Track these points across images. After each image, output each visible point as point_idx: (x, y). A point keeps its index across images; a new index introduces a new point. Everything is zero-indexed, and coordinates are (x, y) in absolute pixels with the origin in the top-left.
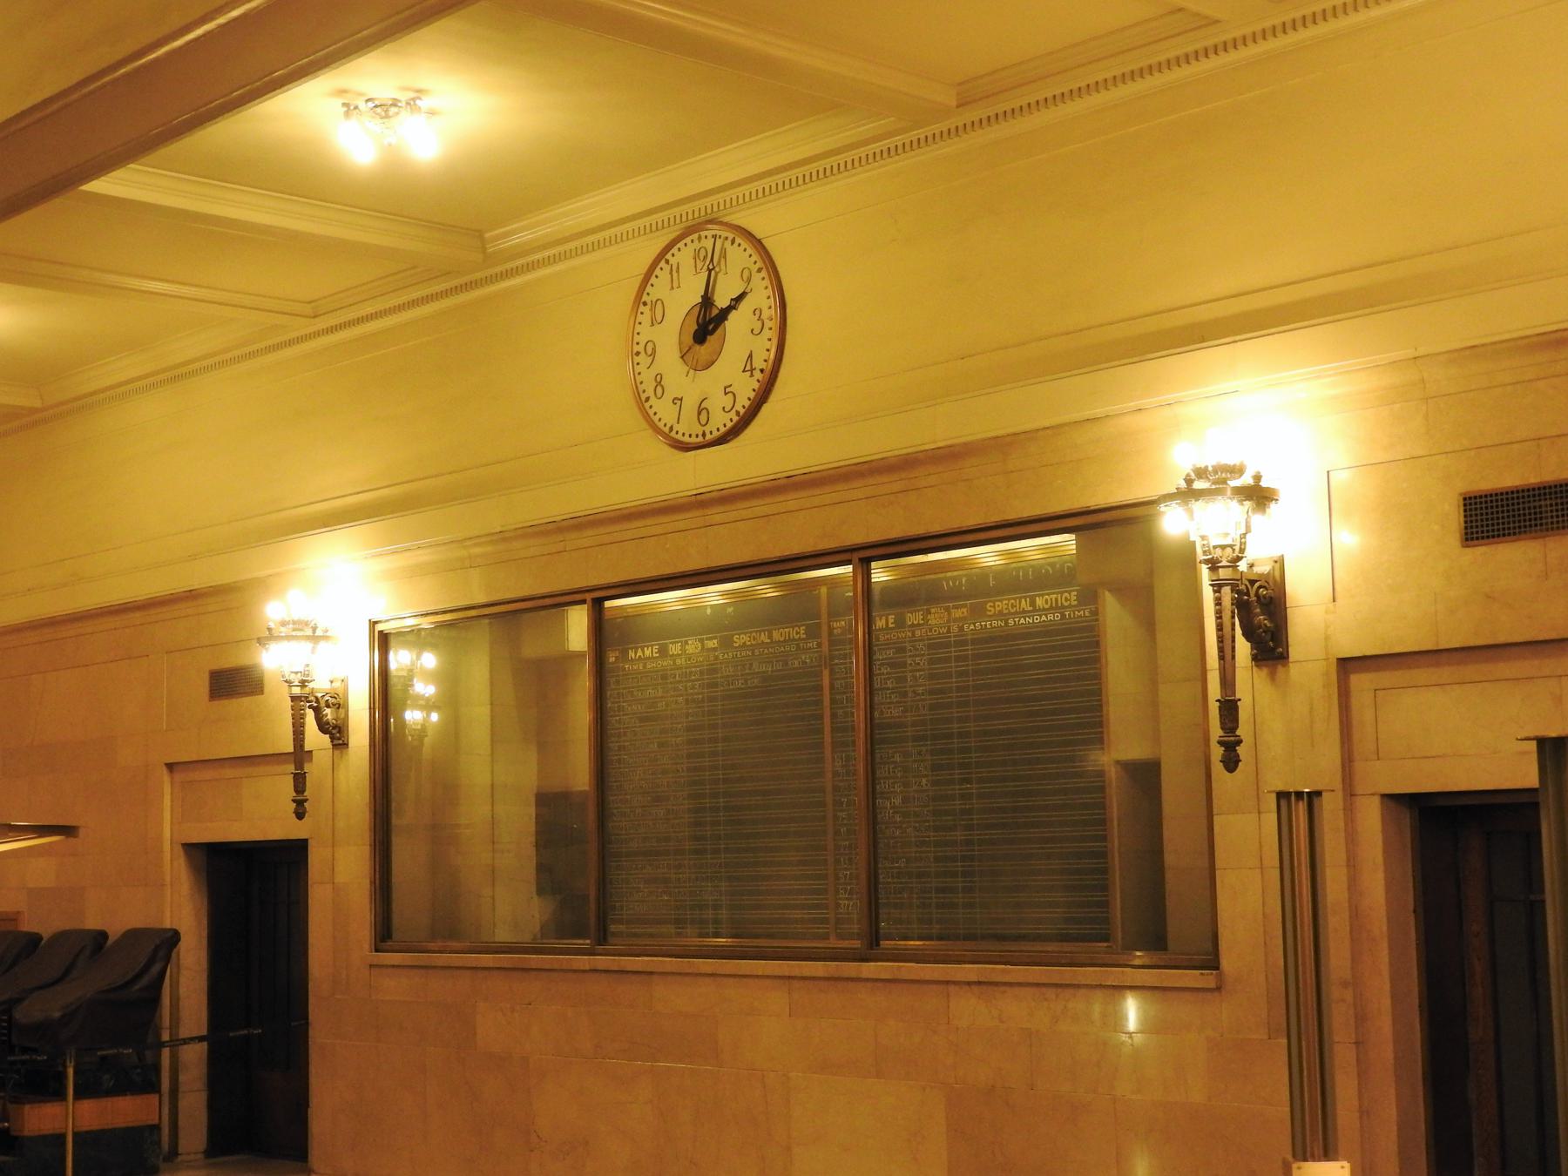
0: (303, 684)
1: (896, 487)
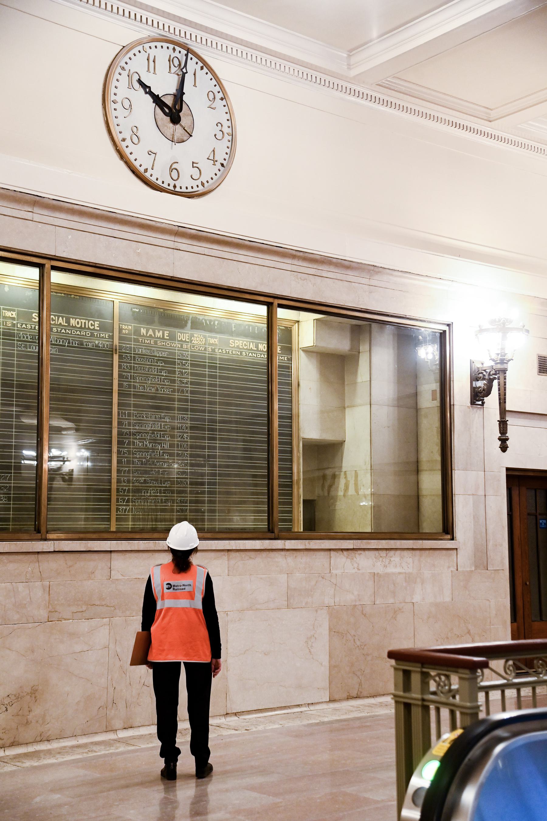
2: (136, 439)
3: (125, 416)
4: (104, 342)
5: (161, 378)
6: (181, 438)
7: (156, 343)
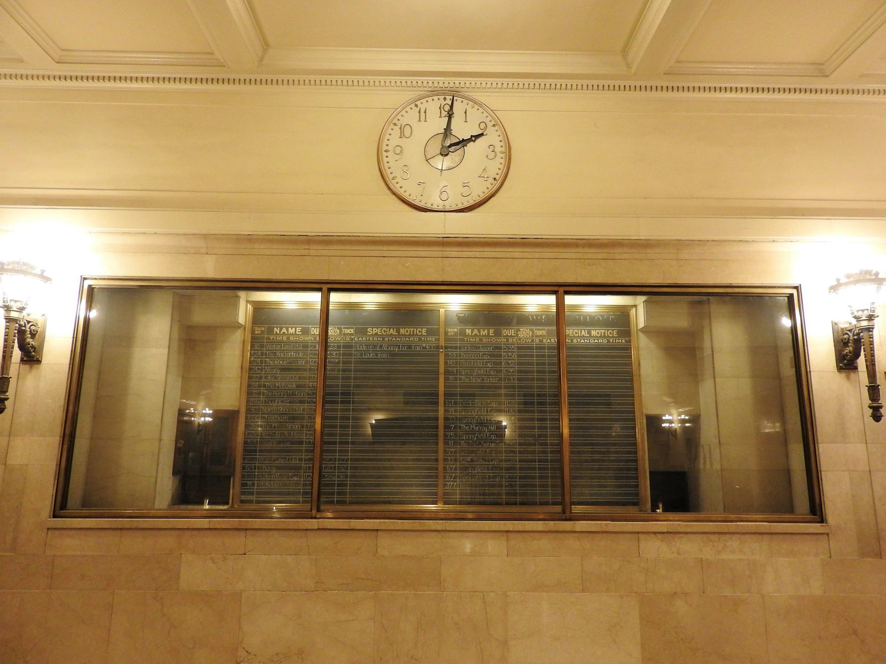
0: (21, 309)
1: (601, 256)
7: (481, 340)
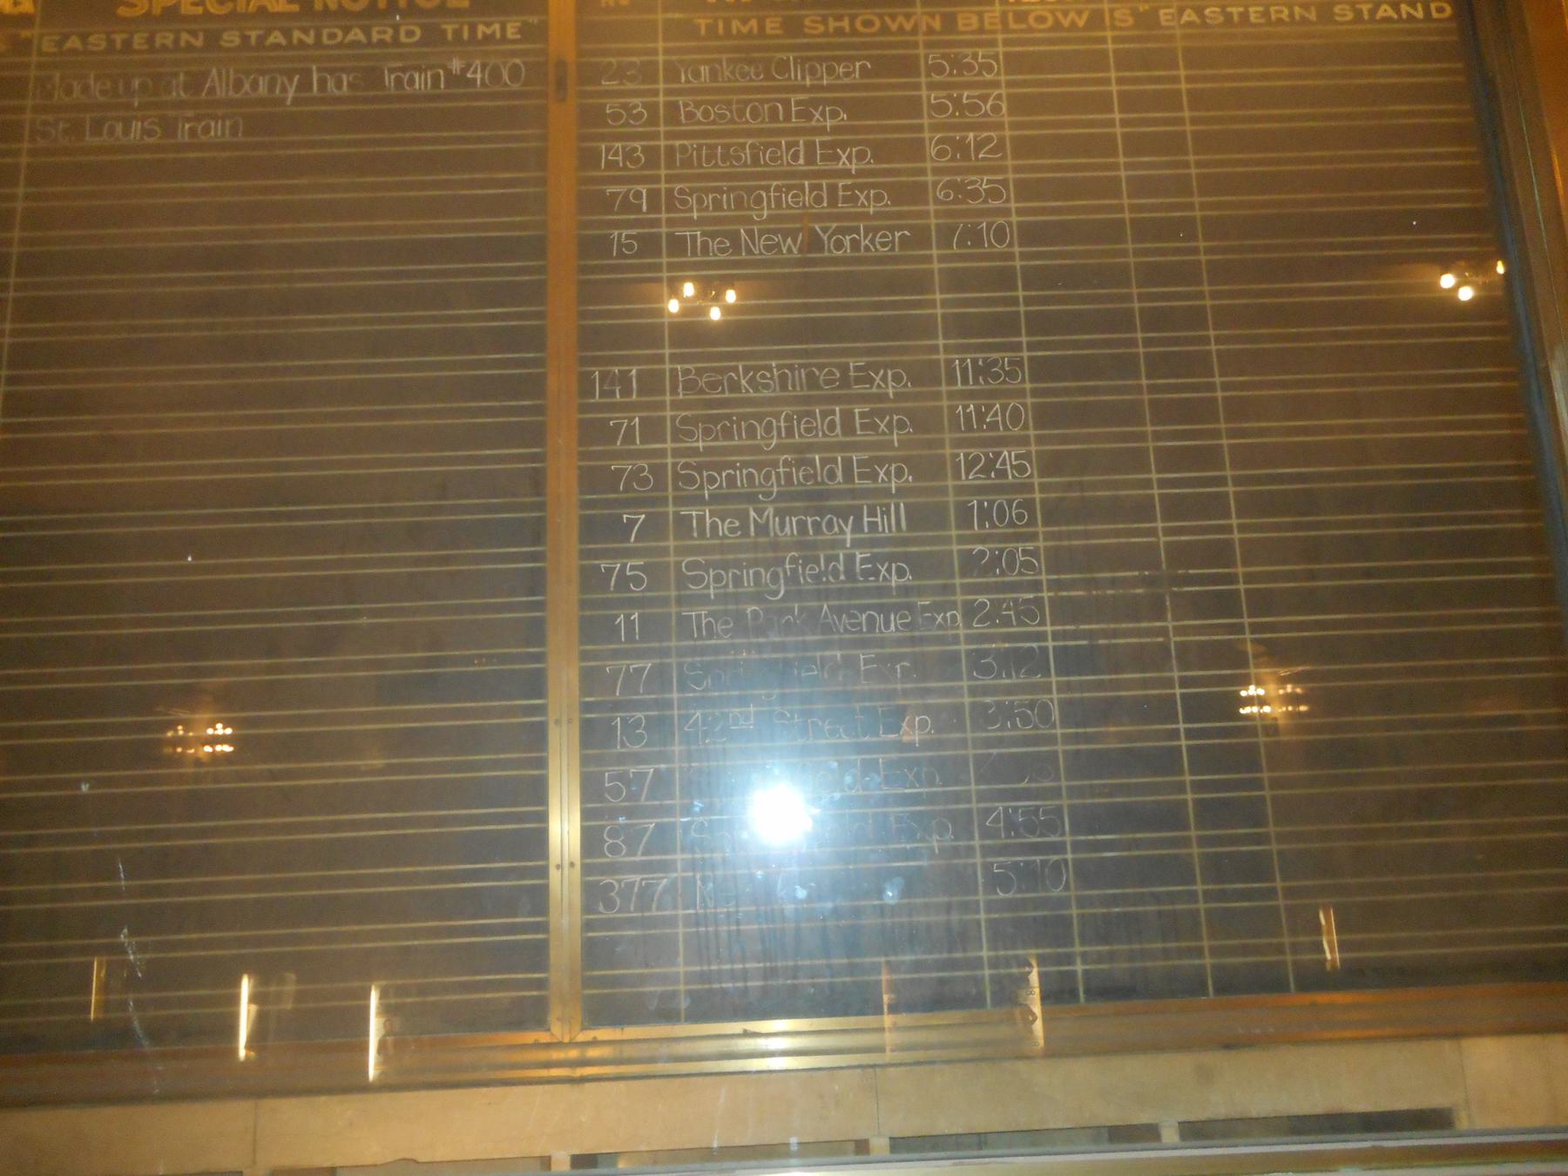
2: (697, 500)
3: (626, 392)
4: (493, 61)
5: (833, 189)
6: (986, 470)
